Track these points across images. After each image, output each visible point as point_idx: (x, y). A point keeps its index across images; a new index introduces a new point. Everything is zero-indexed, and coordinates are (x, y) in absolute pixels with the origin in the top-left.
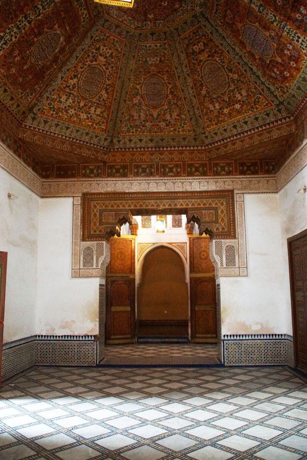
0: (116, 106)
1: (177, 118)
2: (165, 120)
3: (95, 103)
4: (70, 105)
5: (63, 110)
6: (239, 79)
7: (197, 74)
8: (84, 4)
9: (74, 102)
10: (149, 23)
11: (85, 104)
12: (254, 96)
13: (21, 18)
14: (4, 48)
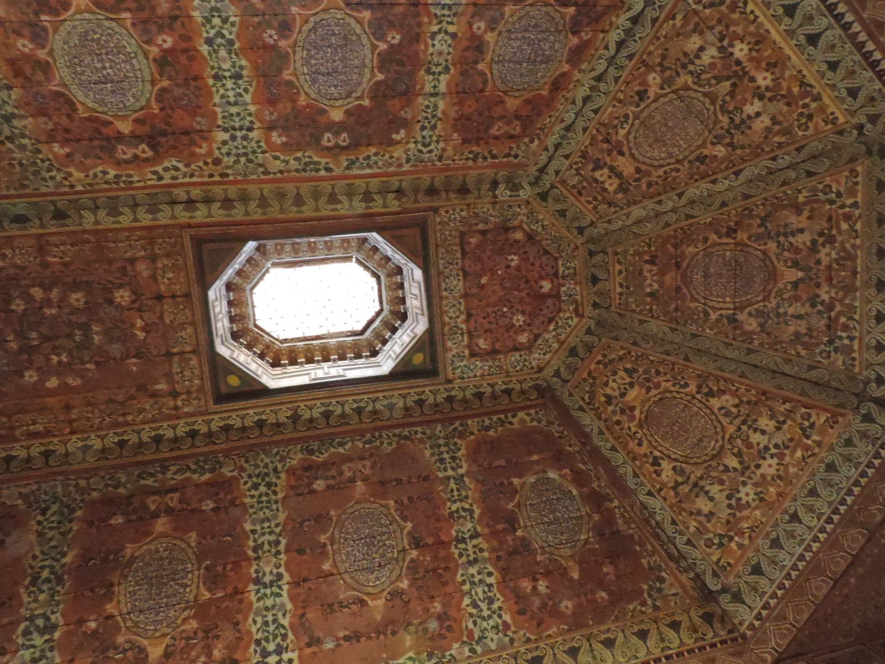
0: (763, 376)
1: (806, 213)
2: (814, 248)
3: (739, 429)
4: (726, 493)
5: (734, 515)
6: (658, 69)
7: (674, 174)
8: (502, 416)
9: (721, 482)
10: (563, 289)
11: (733, 454)
12: (696, 12)
13: (456, 552)
14: (500, 608)
